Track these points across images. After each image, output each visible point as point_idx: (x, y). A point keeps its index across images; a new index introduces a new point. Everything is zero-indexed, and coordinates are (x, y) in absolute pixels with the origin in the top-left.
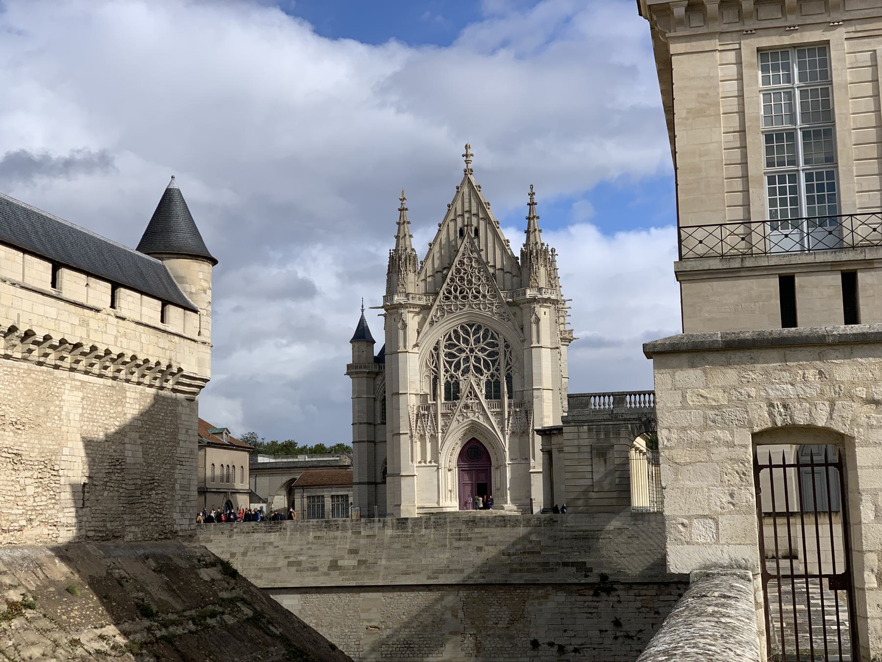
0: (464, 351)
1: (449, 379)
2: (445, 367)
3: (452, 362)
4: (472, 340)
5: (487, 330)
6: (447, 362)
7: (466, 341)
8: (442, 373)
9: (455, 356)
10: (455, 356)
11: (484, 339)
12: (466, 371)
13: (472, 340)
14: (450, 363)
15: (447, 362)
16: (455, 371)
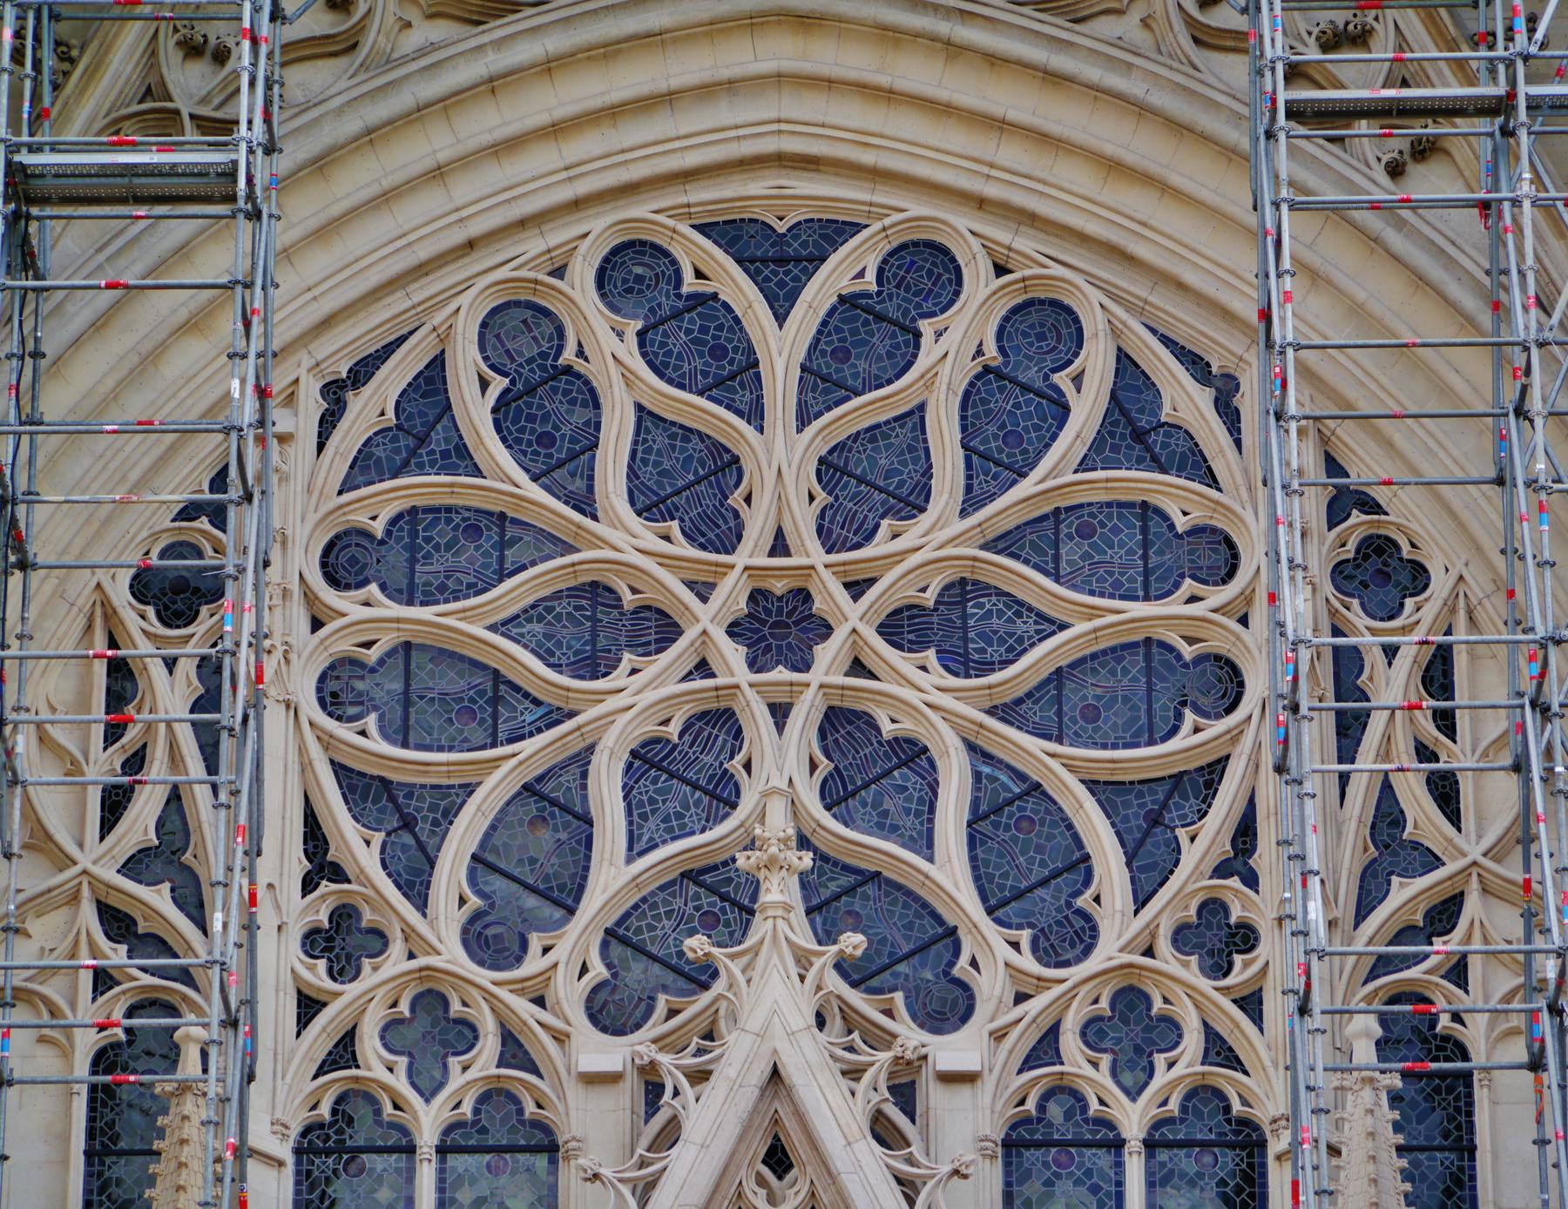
0: (659, 628)
1: (377, 1063)
2: (322, 865)
3: (448, 801)
4: (781, 462)
5: (1044, 325)
6: (361, 788)
7: (693, 487)
8: (282, 962)
9: (494, 706)
10: (494, 706)
11: (992, 465)
12: (660, 966)
13: (781, 462)
14: (408, 817)
15: (361, 788)
16: (491, 941)
